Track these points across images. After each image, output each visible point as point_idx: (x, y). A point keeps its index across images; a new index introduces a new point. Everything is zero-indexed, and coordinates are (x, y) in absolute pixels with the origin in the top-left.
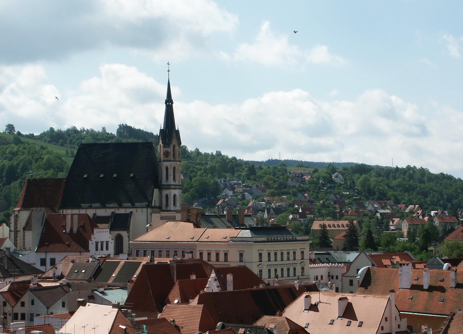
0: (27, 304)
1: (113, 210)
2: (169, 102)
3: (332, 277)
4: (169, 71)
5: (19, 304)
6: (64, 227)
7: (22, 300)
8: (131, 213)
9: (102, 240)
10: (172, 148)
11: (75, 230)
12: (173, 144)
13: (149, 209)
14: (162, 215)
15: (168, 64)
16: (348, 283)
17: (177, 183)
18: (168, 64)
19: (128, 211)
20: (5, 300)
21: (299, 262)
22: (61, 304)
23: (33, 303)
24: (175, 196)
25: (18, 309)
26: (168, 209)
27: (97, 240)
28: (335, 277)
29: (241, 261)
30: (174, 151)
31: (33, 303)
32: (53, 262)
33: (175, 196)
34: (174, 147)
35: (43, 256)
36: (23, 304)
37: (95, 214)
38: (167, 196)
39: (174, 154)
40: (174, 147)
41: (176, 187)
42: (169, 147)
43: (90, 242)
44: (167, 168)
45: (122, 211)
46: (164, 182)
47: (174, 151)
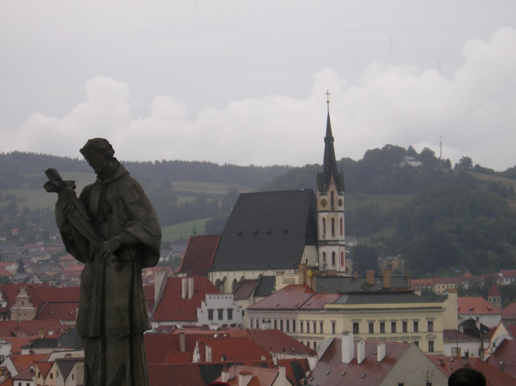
0: (54, 376)
1: (261, 272)
4: (328, 102)
5: (49, 376)
9: (221, 307)
10: (329, 195)
11: (190, 296)
12: (330, 191)
14: (284, 278)
15: (328, 94)
18: (328, 94)
21: (424, 336)
24: (334, 254)
27: (210, 307)
29: (334, 332)
33: (334, 254)
34: (332, 193)
37: (243, 277)
38: (324, 254)
40: (332, 193)
41: (335, 243)
42: (326, 195)
43: (199, 310)
44: (324, 220)
45: (269, 273)
46: (321, 238)
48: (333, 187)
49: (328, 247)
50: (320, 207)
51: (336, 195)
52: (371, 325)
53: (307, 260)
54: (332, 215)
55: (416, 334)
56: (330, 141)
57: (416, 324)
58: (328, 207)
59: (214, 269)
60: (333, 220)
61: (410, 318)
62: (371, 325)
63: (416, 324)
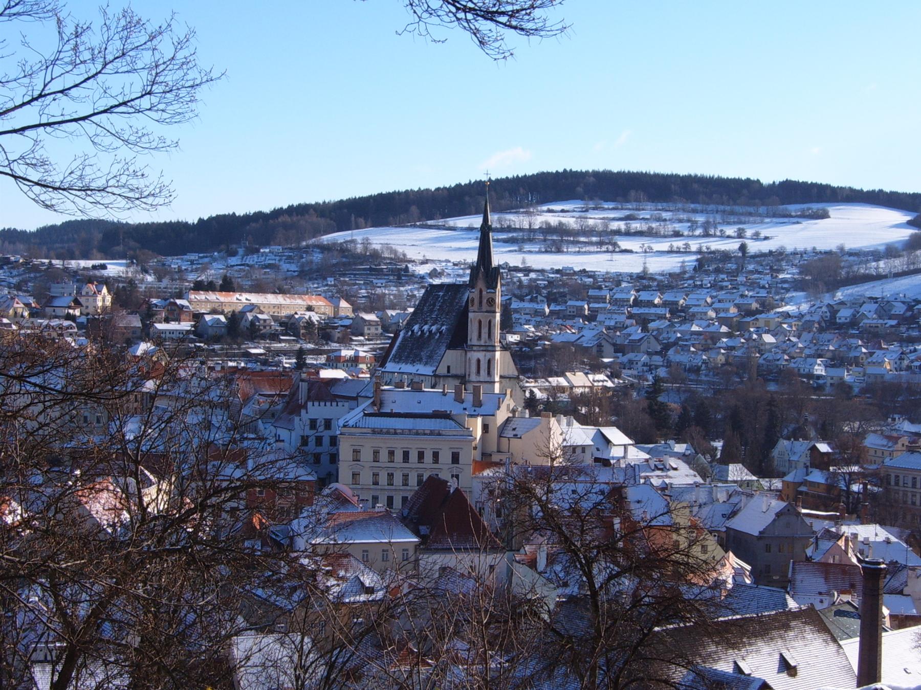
17: (482, 343)
24: (479, 361)
30: (481, 297)
33: (479, 361)
34: (481, 291)
39: (481, 302)
40: (481, 291)
47: (481, 297)
48: (481, 284)
50: (471, 308)
51: (484, 293)
52: (376, 453)
53: (449, 367)
54: (479, 316)
55: (436, 466)
57: (436, 455)
58: (476, 307)
60: (480, 322)
61: (429, 446)
62: (376, 453)
63: (436, 455)
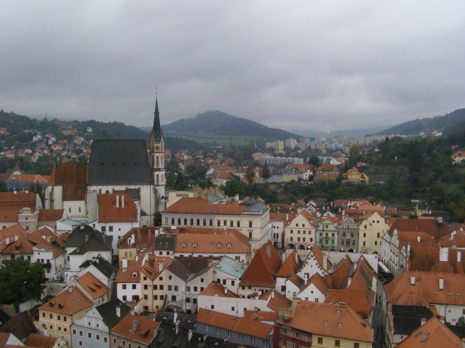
1: (127, 186)
2: (157, 114)
3: (274, 227)
5: (158, 278)
6: (114, 203)
7: (161, 275)
8: (140, 188)
11: (123, 205)
13: (151, 186)
16: (290, 232)
19: (137, 187)
20: (145, 276)
22: (200, 280)
23: (170, 278)
25: (157, 282)
26: (159, 184)
28: (276, 228)
31: (170, 278)
32: (111, 229)
35: (103, 225)
36: (161, 279)
38: (158, 175)
44: (157, 157)
45: (132, 187)
46: (155, 167)
49: (160, 172)
56: (157, 114)
59: (90, 185)
